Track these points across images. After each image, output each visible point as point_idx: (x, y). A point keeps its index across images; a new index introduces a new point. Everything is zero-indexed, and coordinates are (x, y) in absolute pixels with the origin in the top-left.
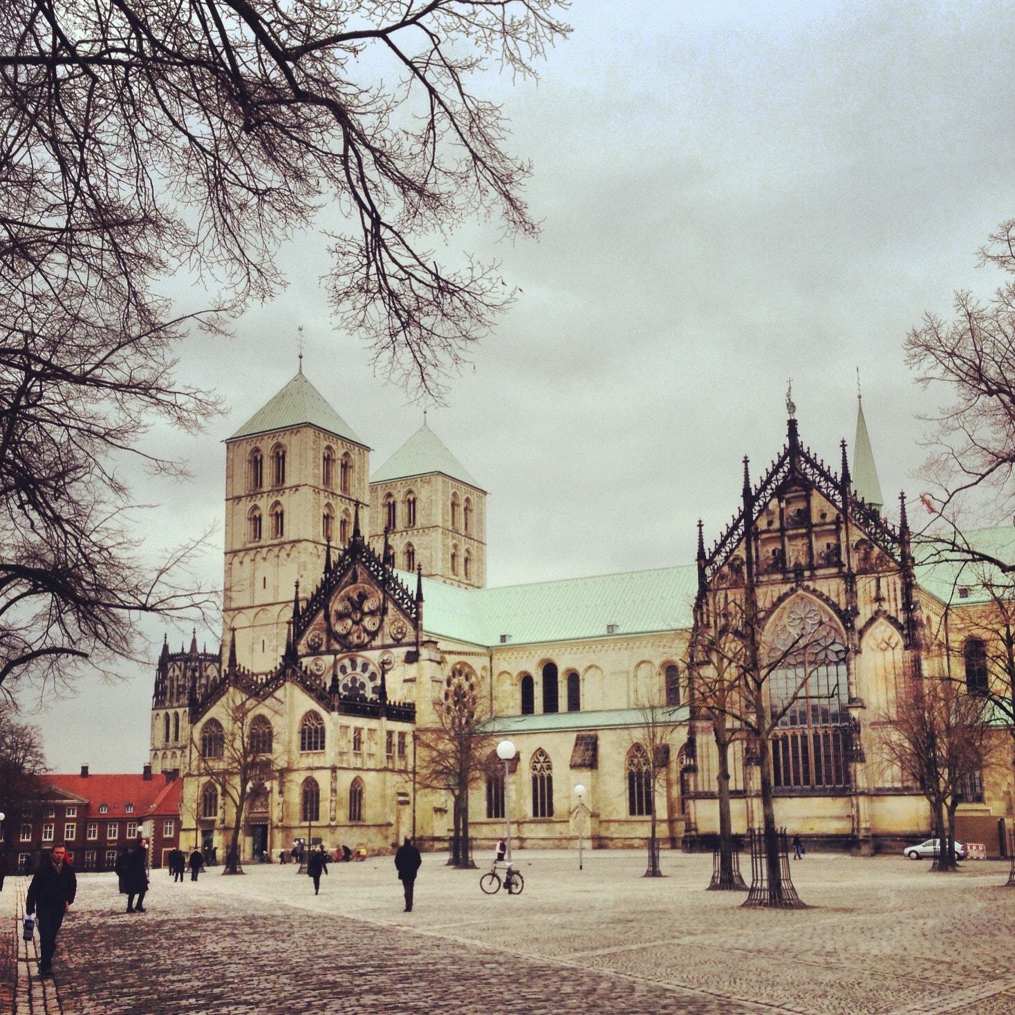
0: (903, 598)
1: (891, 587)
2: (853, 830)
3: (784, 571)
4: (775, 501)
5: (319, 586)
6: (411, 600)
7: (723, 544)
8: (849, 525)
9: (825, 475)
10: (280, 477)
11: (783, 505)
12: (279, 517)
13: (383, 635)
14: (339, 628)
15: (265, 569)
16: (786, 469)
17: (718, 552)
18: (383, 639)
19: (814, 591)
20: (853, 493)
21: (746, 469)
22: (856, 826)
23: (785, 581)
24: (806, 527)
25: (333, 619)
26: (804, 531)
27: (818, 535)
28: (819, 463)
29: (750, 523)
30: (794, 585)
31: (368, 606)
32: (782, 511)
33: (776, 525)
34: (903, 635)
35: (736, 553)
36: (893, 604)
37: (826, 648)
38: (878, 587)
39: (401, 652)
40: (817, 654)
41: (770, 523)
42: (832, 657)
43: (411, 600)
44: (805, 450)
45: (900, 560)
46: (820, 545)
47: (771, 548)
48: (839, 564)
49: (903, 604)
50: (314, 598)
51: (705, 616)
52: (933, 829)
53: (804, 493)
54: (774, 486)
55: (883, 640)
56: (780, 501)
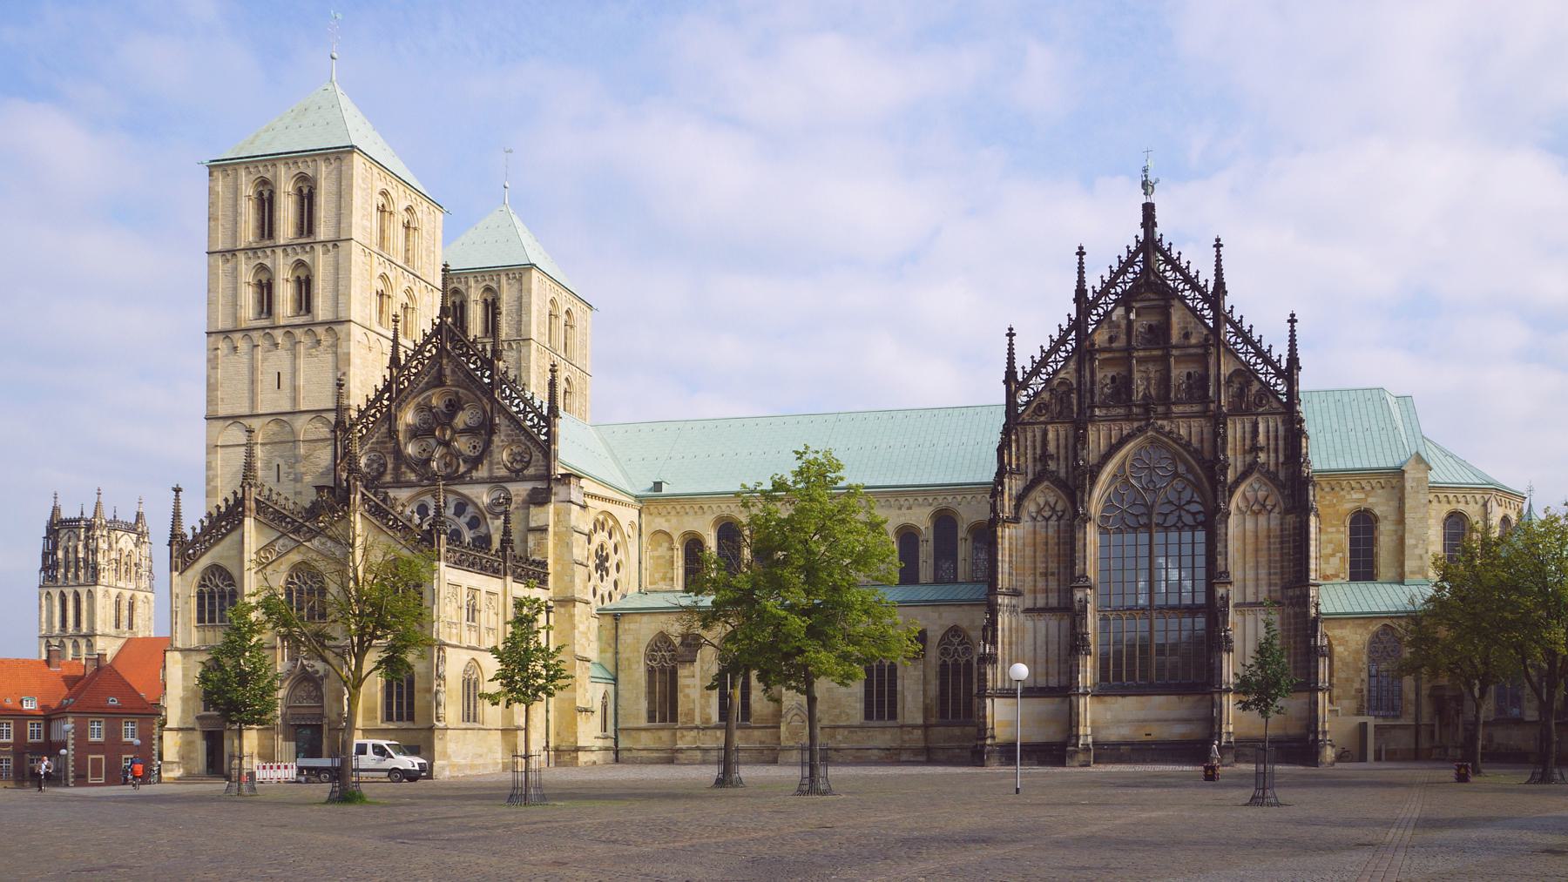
0: (1285, 449)
1: (1272, 435)
4: (1120, 311)
5: (380, 387)
6: (540, 416)
7: (1043, 362)
8: (1222, 349)
9: (1191, 282)
10: (306, 224)
11: (1132, 316)
12: (304, 287)
13: (491, 463)
14: (411, 449)
15: (274, 362)
16: (1137, 269)
17: (1035, 372)
18: (490, 470)
20: (1227, 309)
23: (1128, 418)
24: (1162, 349)
25: (401, 437)
28: (1184, 265)
29: (1082, 336)
30: (1143, 423)
31: (462, 420)
32: (1130, 323)
33: (1121, 343)
35: (1062, 375)
36: (1272, 455)
37: (1180, 507)
39: (519, 490)
40: (1166, 515)
41: (1111, 340)
42: (1188, 519)
43: (540, 416)
44: (1166, 247)
45: (1285, 400)
46: (1178, 373)
47: (1111, 372)
48: (1204, 399)
50: (371, 404)
53: (1162, 303)
54: (1119, 290)
55: (1256, 500)
56: (1128, 311)
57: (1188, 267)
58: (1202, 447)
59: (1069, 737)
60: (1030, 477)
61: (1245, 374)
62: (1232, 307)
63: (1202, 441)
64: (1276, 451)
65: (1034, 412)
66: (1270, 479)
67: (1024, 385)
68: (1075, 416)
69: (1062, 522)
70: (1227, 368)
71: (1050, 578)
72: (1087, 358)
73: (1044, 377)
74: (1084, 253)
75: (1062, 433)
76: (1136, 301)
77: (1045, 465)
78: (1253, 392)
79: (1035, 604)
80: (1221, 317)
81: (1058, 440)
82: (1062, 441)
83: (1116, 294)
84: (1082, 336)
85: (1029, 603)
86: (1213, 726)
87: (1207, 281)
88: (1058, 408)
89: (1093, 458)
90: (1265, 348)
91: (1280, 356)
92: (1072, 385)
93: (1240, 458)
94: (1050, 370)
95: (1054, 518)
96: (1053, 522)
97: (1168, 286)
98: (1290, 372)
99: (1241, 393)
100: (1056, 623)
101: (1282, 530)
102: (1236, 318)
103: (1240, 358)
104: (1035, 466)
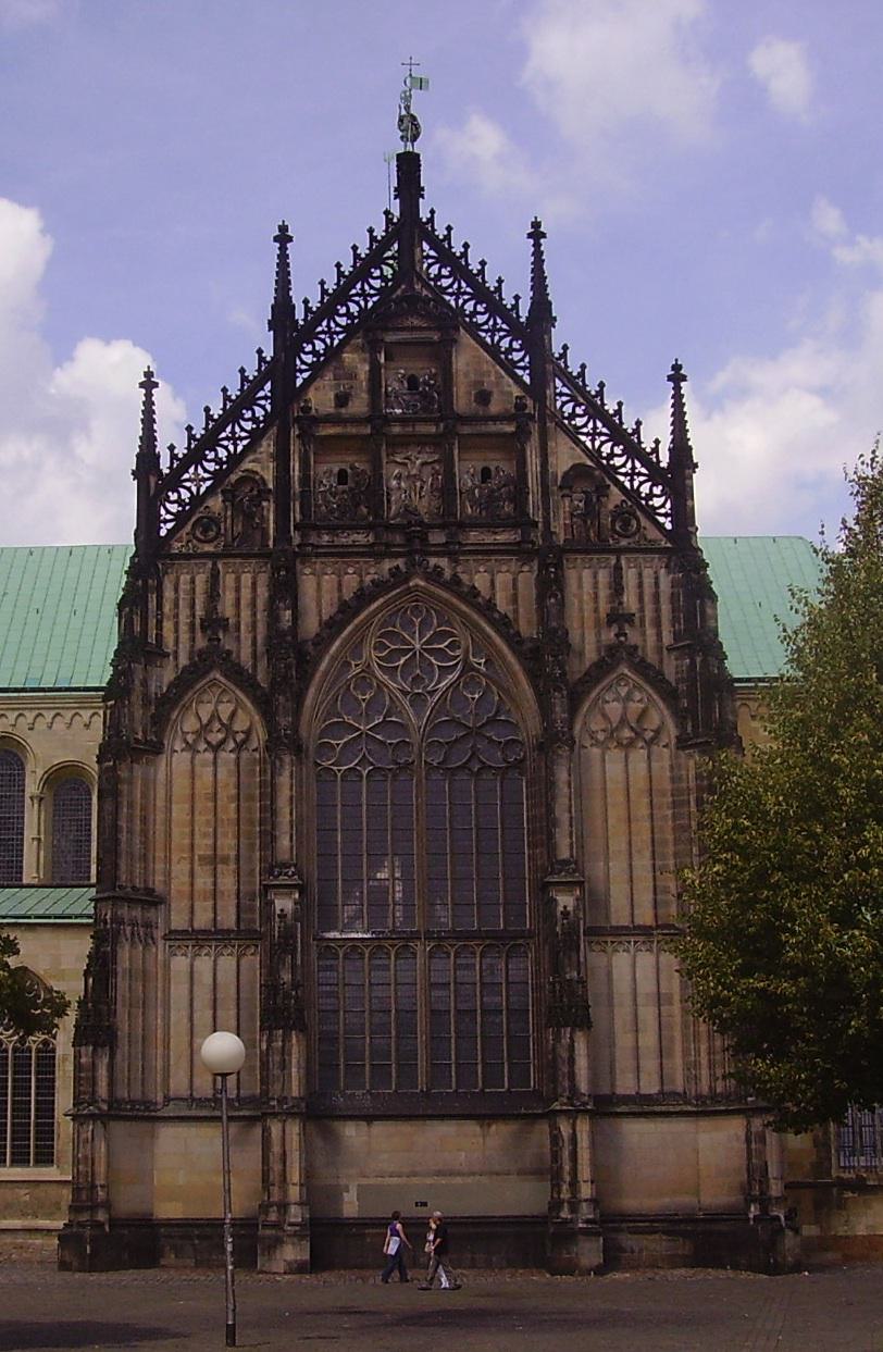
0: (674, 620)
1: (648, 591)
2: (556, 1205)
3: (378, 525)
7: (210, 440)
9: (489, 298)
17: (195, 456)
19: (456, 580)
20: (557, 350)
21: (283, 258)
22: (565, 1195)
23: (375, 553)
24: (436, 422)
26: (433, 429)
27: (471, 444)
28: (475, 267)
29: (287, 395)
30: (400, 562)
33: (359, 405)
34: (680, 716)
35: (247, 465)
36: (650, 631)
37: (471, 733)
38: (617, 588)
41: (342, 400)
44: (441, 232)
45: (669, 526)
46: (466, 471)
48: (521, 521)
49: (677, 636)
51: (152, 622)
52: (749, 1199)
54: (354, 308)
55: (623, 721)
56: (373, 347)
57: (482, 272)
58: (516, 611)
59: (264, 1208)
60: (183, 661)
61: (593, 476)
62: (565, 348)
63: (514, 599)
64: (657, 623)
65: (192, 533)
66: (648, 680)
67: (174, 481)
68: (271, 543)
69: (244, 755)
70: (564, 458)
71: (219, 866)
72: (294, 431)
73: (211, 467)
74: (290, 239)
75: (246, 579)
76: (386, 329)
77: (214, 639)
78: (611, 507)
79: (192, 920)
80: (546, 365)
81: (238, 590)
82: (246, 594)
83: (348, 315)
84: (287, 395)
85: (179, 921)
86: (556, 1187)
87: (517, 298)
88: (239, 528)
89: (311, 625)
90: (629, 425)
91: (657, 442)
92: (264, 482)
93: (590, 638)
94: (222, 453)
95: (232, 745)
96: (227, 756)
97: (447, 304)
98: (678, 472)
99: (591, 512)
100: (232, 961)
101: (673, 780)
102: (574, 370)
103: (584, 443)
104: (193, 639)
